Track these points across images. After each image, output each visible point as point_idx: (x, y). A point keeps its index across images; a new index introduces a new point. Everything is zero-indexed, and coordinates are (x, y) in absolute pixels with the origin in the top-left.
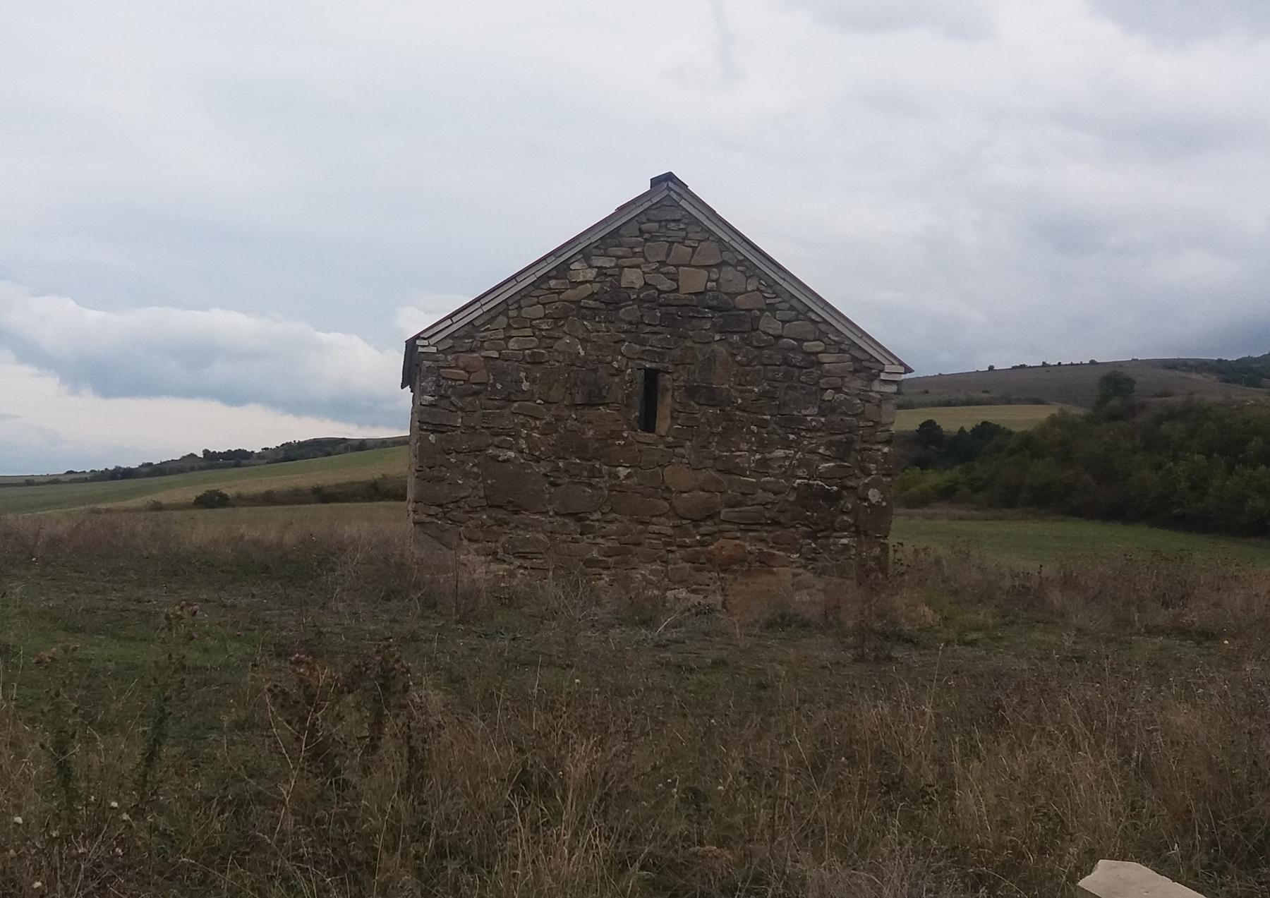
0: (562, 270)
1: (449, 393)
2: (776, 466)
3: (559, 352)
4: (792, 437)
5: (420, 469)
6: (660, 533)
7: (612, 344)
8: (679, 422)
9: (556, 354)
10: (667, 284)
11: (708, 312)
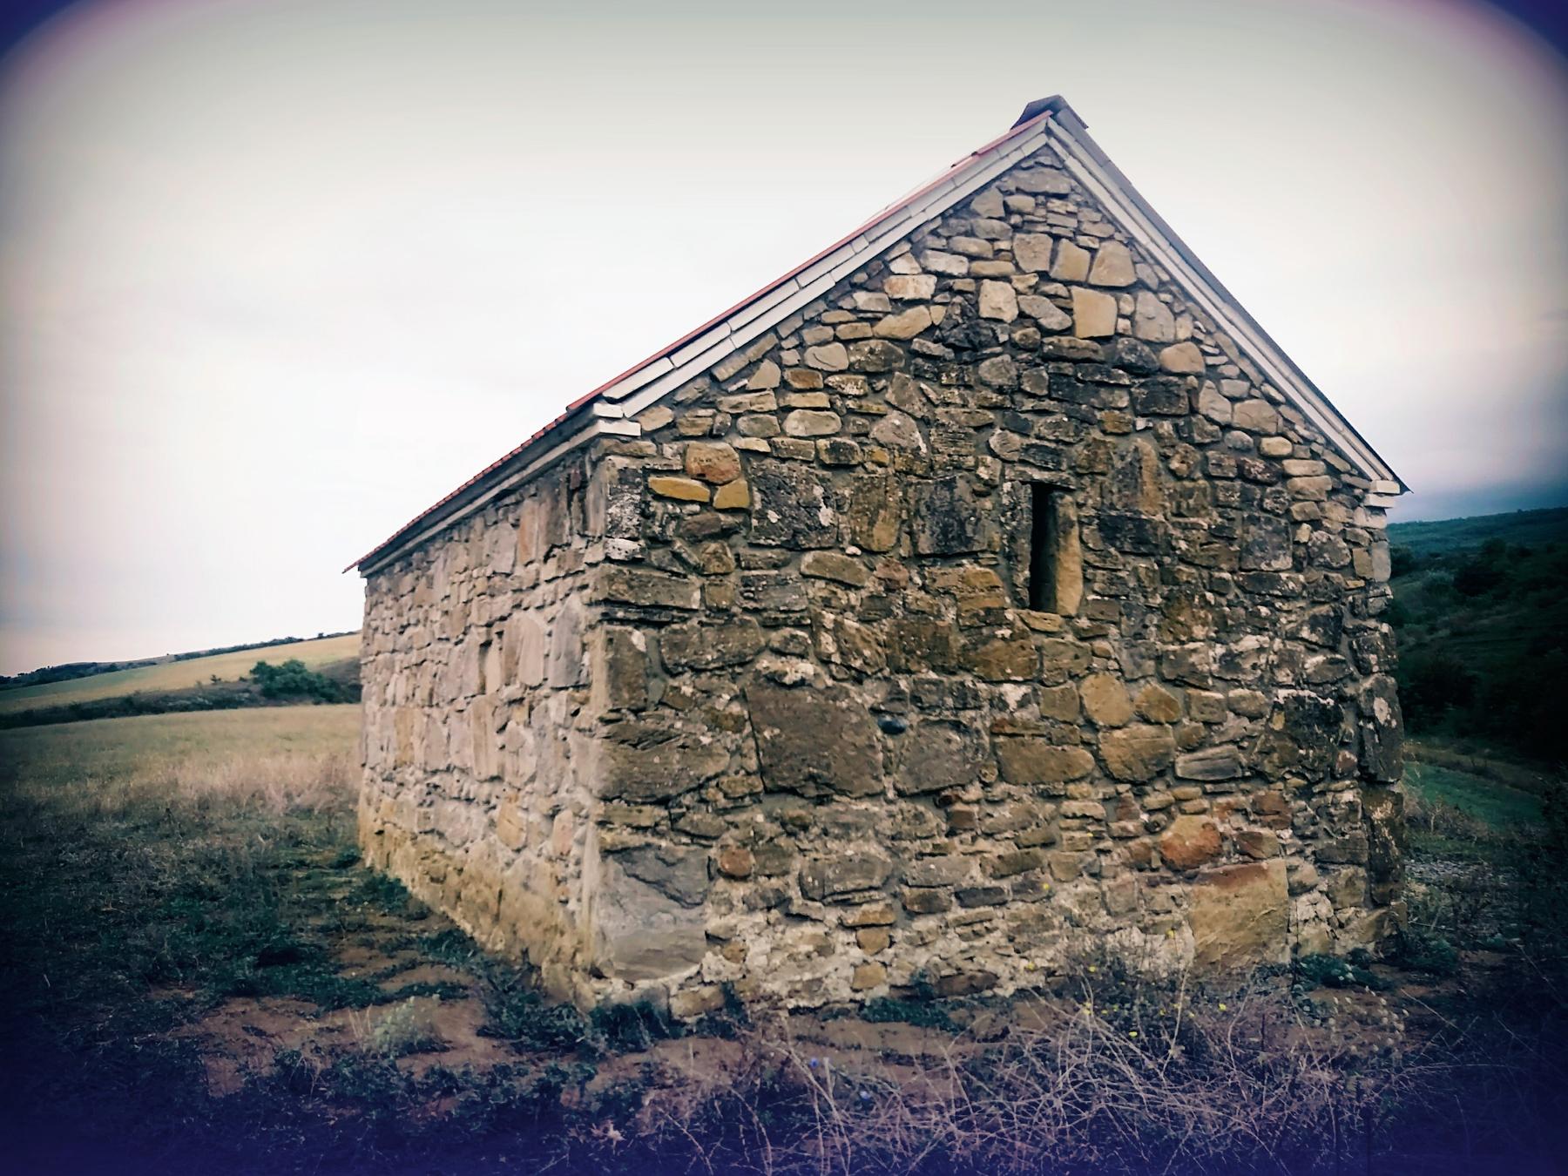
0: (877, 271)
1: (670, 532)
2: (1247, 666)
3: (882, 446)
4: (1264, 610)
5: (613, 716)
6: (1084, 816)
7: (971, 431)
8: (1096, 587)
9: (876, 449)
10: (1054, 319)
11: (1122, 375)
